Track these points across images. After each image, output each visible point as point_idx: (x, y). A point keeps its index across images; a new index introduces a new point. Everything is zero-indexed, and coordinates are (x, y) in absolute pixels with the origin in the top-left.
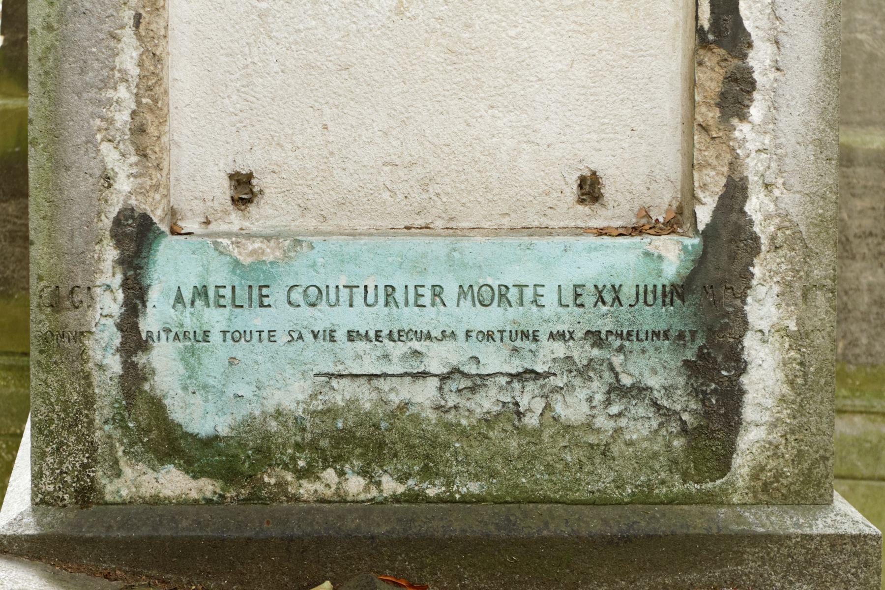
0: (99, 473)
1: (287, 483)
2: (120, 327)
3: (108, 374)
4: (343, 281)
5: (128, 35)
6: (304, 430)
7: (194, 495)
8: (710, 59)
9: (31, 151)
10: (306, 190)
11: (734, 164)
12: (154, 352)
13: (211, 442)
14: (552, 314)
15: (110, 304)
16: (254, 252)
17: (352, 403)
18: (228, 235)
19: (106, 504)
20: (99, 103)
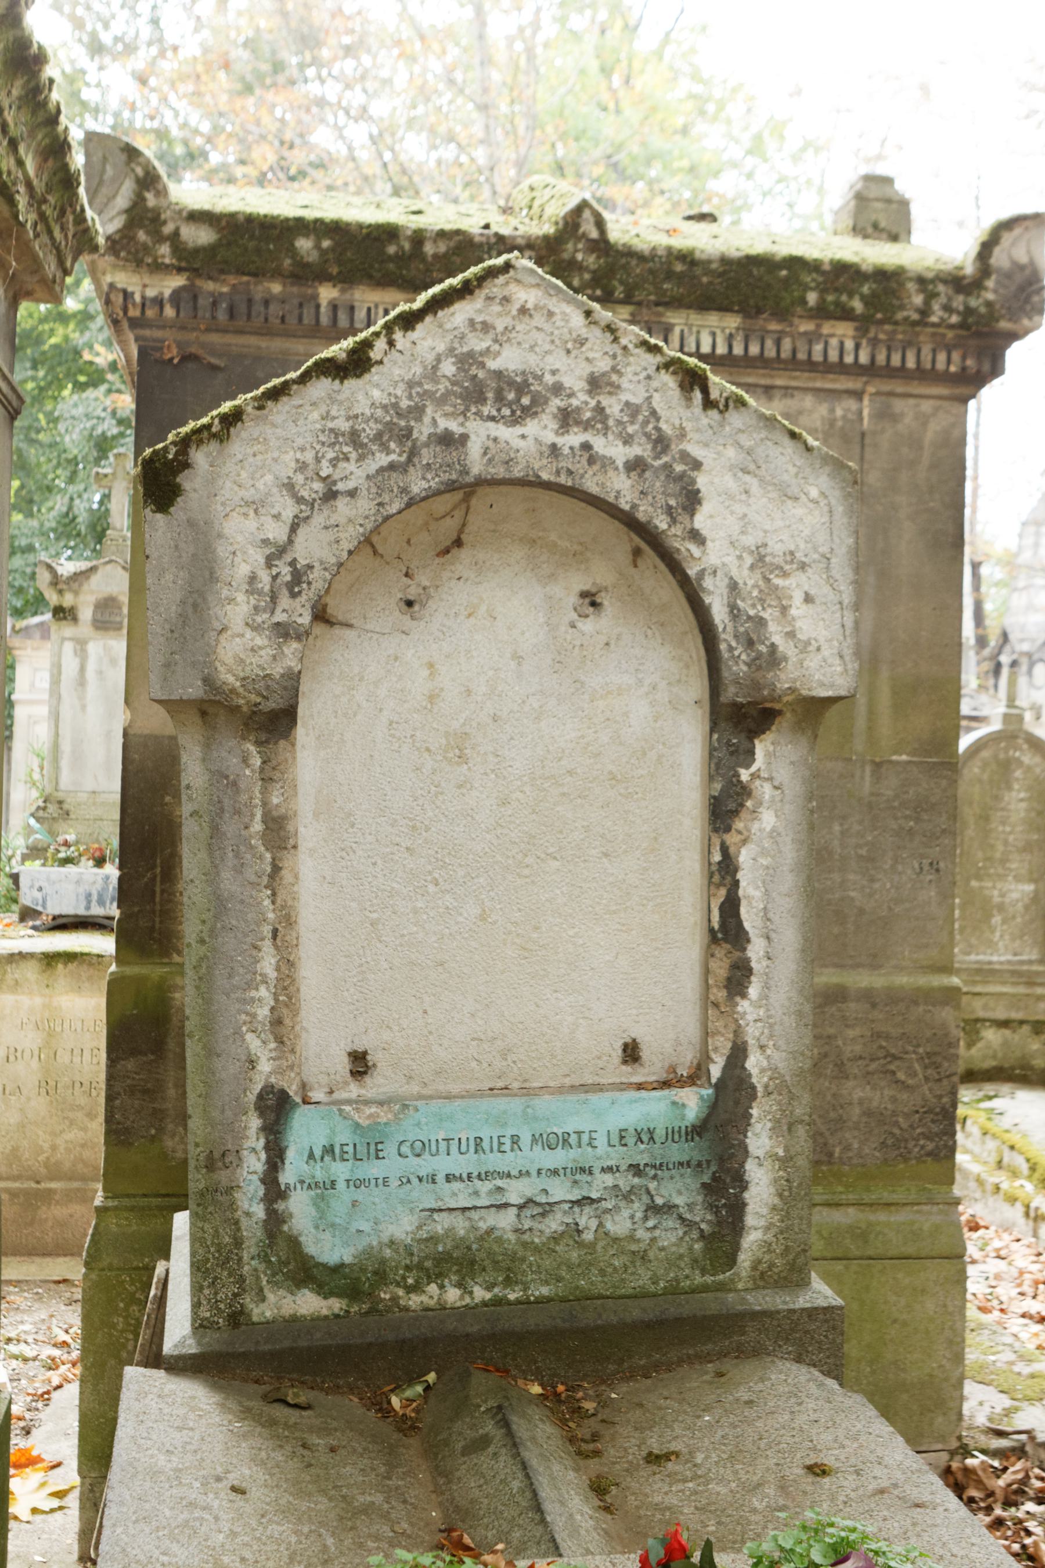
0: (247, 1300)
1: (399, 1297)
2: (263, 1181)
3: (254, 1219)
4: (441, 1135)
5: (267, 946)
6: (412, 1254)
7: (325, 1312)
8: (719, 952)
9: (188, 1042)
10: (411, 1063)
11: (738, 1032)
12: (292, 1200)
13: (338, 1269)
14: (604, 1153)
15: (255, 1163)
16: (371, 1116)
17: (450, 1231)
18: (349, 1102)
19: (253, 1324)
20: (244, 1001)
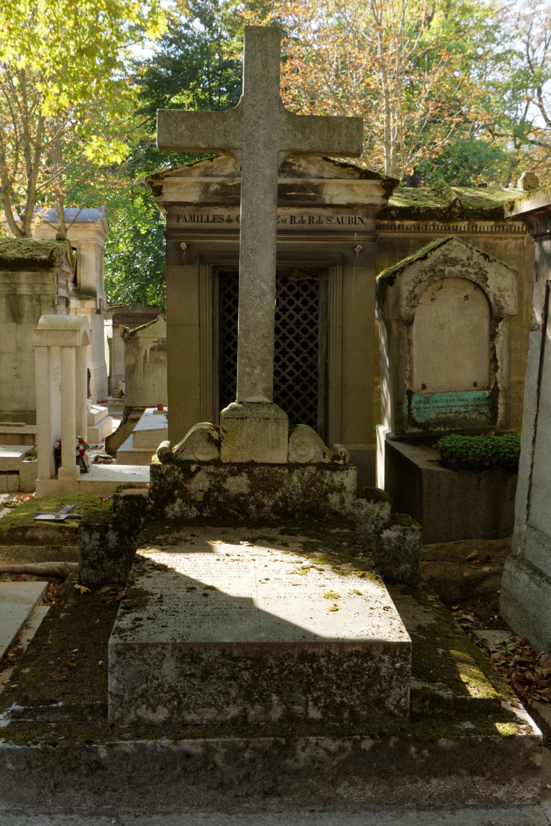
13: (421, 424)
15: (406, 404)
